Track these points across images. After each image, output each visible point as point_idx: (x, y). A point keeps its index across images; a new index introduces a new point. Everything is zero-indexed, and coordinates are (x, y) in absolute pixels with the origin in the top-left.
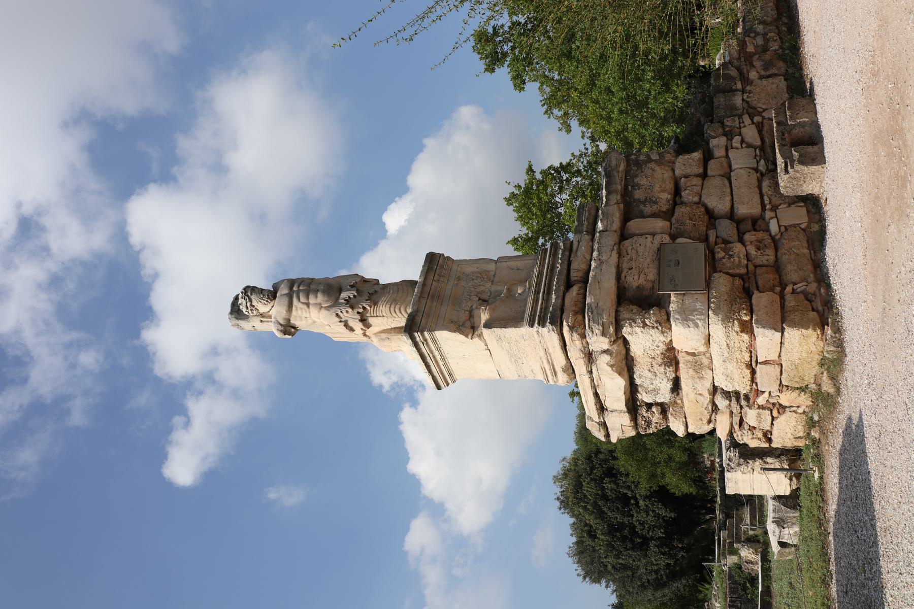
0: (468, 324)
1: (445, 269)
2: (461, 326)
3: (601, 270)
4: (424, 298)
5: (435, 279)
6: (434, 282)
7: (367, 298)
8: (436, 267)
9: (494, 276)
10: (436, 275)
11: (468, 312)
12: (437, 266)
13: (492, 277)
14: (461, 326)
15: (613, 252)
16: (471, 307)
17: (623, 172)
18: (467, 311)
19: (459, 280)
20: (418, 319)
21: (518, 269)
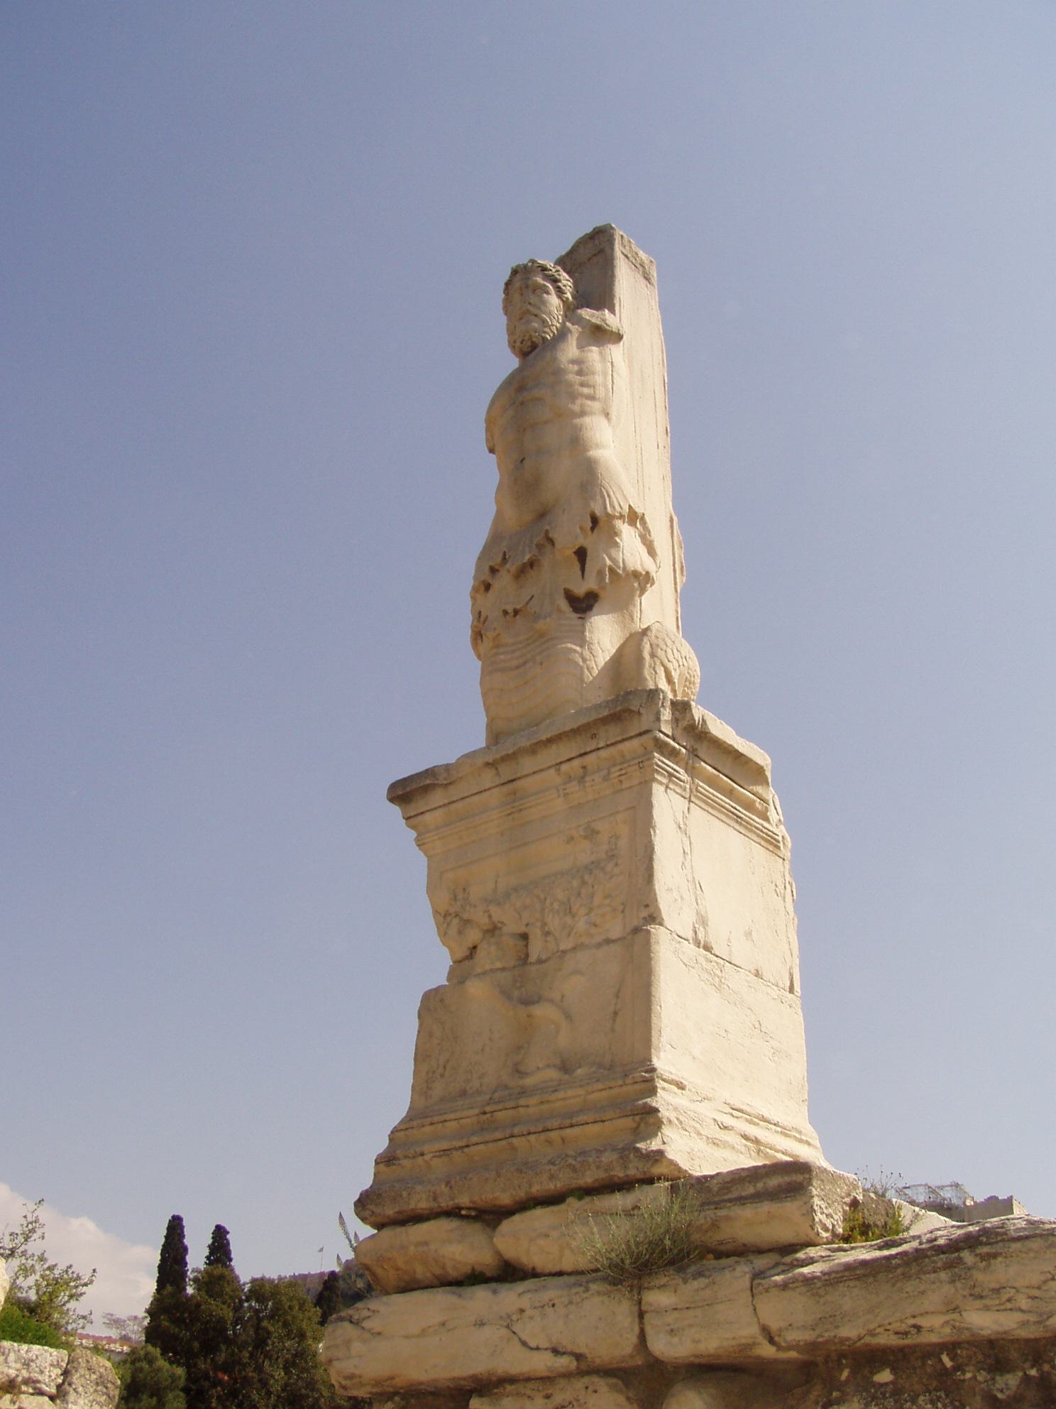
0: (473, 936)
1: (609, 773)
2: (461, 919)
3: (482, 1324)
4: (498, 774)
5: (564, 767)
6: (552, 771)
7: (510, 609)
8: (601, 745)
9: (608, 941)
10: (576, 763)
11: (486, 920)
12: (608, 746)
13: (598, 939)
14: (461, 919)
15: (549, 1355)
16: (502, 923)
17: (960, 1330)
18: (490, 916)
19: (585, 837)
20: (437, 798)
21: (616, 1014)
